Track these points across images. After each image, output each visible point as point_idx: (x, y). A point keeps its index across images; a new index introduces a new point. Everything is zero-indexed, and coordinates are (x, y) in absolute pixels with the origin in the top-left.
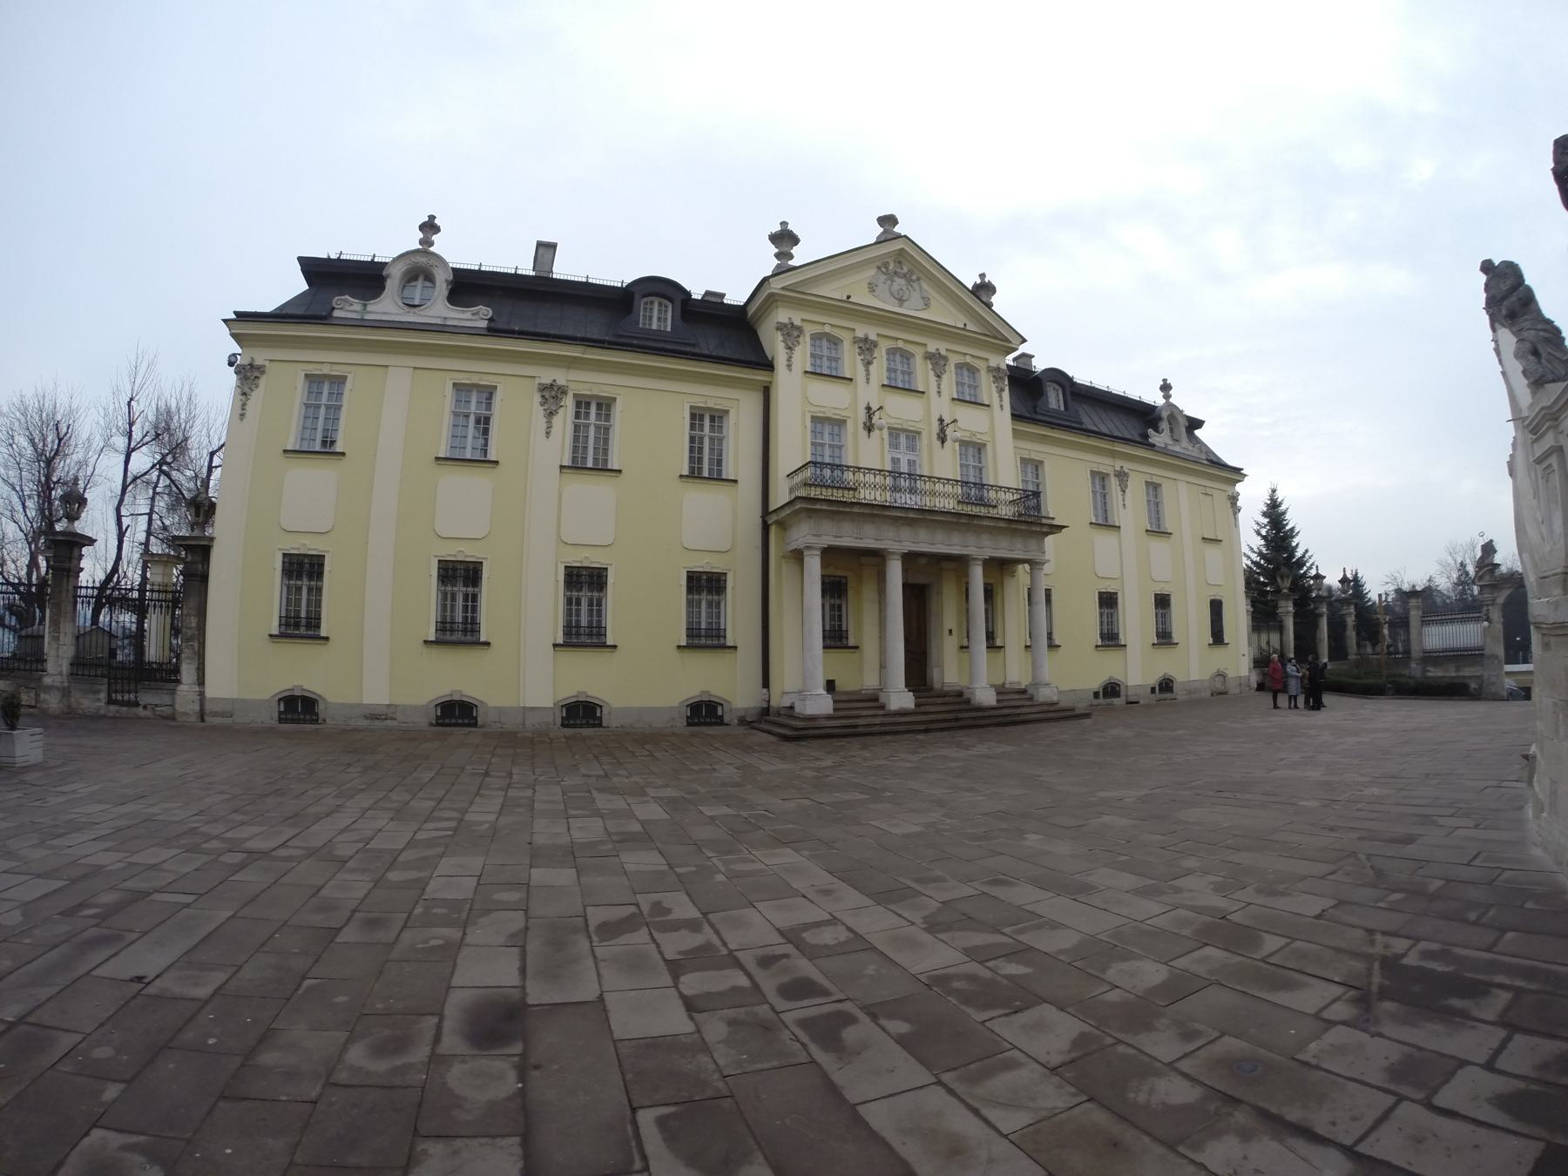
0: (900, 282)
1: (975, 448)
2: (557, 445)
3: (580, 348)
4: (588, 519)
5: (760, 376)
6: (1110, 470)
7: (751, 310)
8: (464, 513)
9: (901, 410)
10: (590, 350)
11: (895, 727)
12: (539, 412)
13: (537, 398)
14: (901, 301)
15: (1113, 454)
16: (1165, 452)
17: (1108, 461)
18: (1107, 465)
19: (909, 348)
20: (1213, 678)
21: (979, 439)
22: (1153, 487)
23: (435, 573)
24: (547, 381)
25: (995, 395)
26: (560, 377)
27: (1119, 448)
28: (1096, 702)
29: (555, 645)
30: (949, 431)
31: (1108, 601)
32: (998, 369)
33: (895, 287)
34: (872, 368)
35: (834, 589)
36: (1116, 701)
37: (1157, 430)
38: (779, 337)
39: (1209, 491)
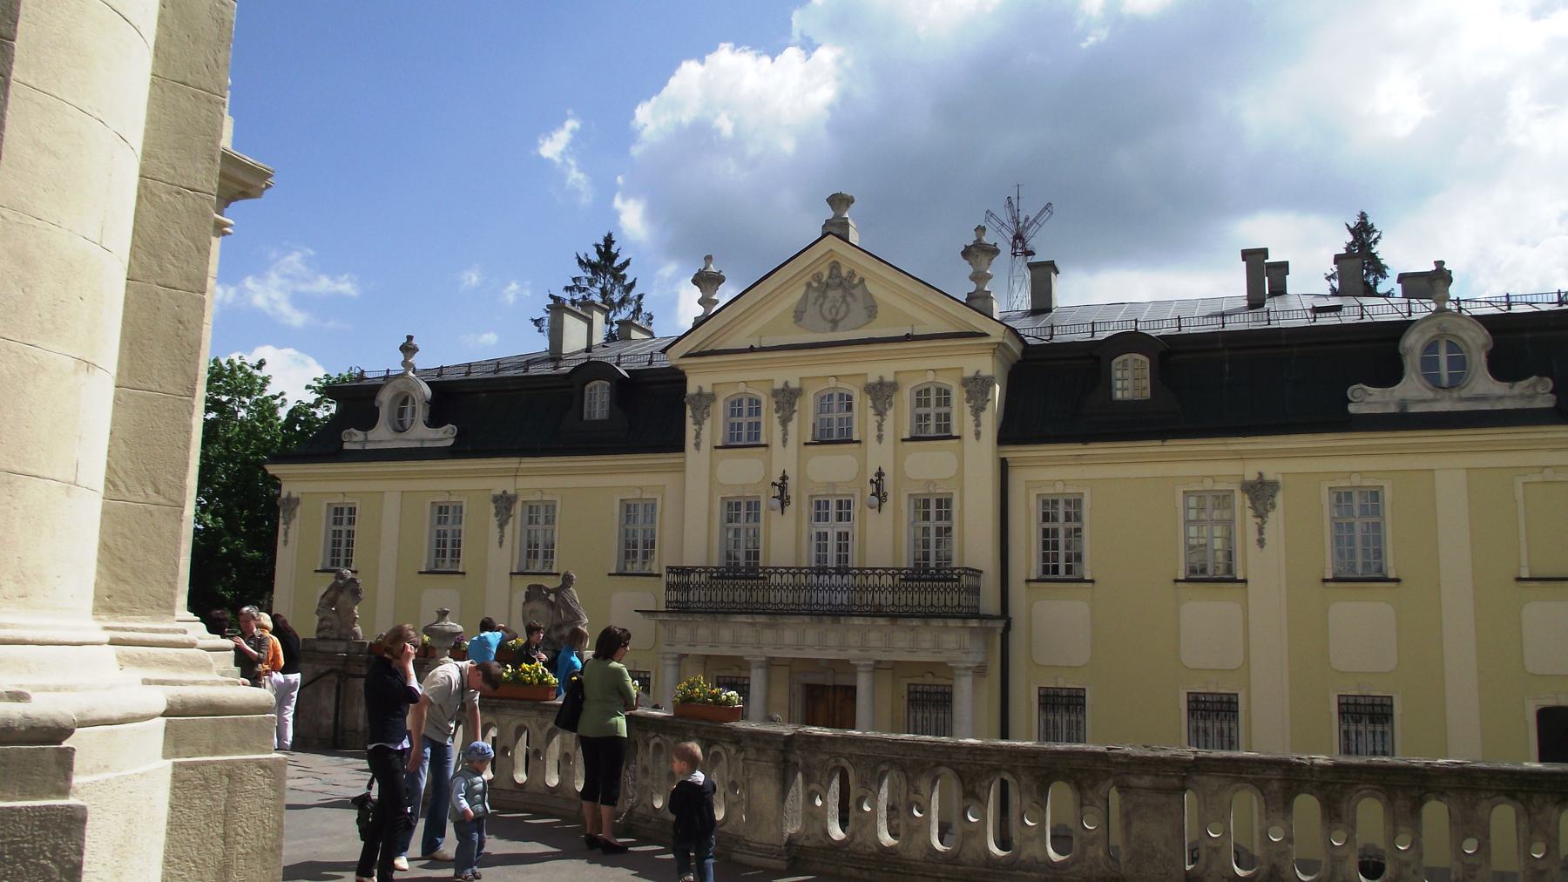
9: (833, 469)
12: (494, 522)
13: (493, 510)
15: (1240, 457)
17: (1233, 468)
19: (846, 386)
21: (941, 490)
24: (499, 492)
33: (827, 305)
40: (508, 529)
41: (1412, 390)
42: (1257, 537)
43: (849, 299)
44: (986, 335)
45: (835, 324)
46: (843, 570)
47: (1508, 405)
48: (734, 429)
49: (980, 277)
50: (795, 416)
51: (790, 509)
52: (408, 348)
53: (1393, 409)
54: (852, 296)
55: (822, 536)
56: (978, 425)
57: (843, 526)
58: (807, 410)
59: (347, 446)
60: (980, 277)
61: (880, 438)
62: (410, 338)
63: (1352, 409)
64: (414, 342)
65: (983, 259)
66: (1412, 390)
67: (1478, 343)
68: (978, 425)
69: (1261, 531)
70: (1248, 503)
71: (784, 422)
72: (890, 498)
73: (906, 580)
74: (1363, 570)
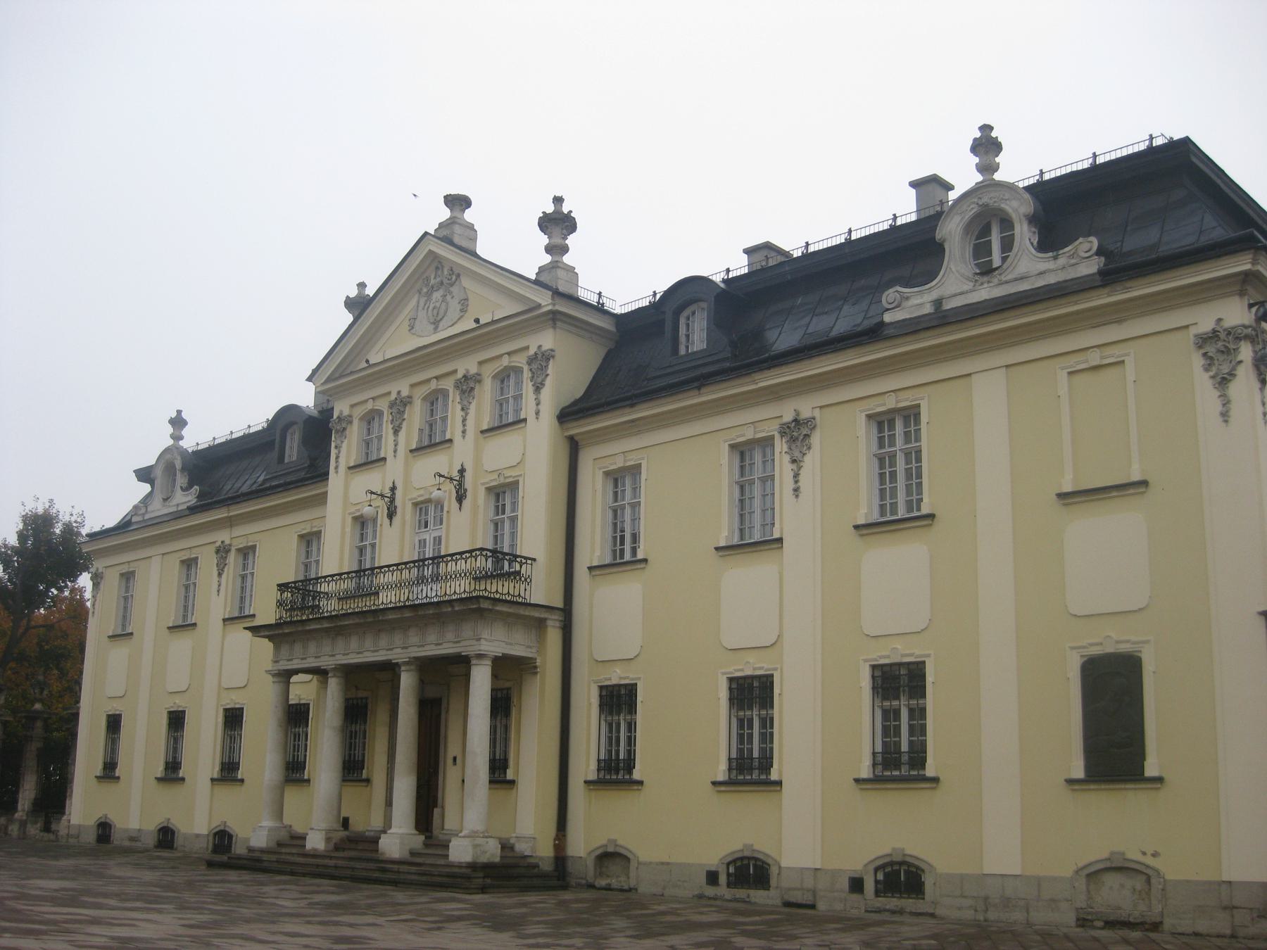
0: (437, 295)
3: (225, 509)
6: (772, 429)
10: (232, 508)
12: (215, 573)
16: (941, 319)
18: (763, 419)
20: (1094, 875)
23: (724, 694)
28: (710, 891)
29: (212, 780)
31: (752, 694)
34: (402, 434)
36: (758, 896)
41: (956, 283)
42: (791, 485)
43: (448, 297)
44: (539, 306)
45: (436, 324)
47: (1051, 279)
49: (556, 250)
50: (404, 424)
51: (397, 520)
52: (178, 422)
53: (928, 309)
54: (450, 293)
55: (422, 543)
58: (416, 416)
60: (556, 250)
62: (179, 412)
64: (184, 415)
65: (557, 231)
66: (956, 283)
67: (1019, 209)
69: (796, 476)
70: (785, 448)
71: (396, 432)
74: (899, 512)
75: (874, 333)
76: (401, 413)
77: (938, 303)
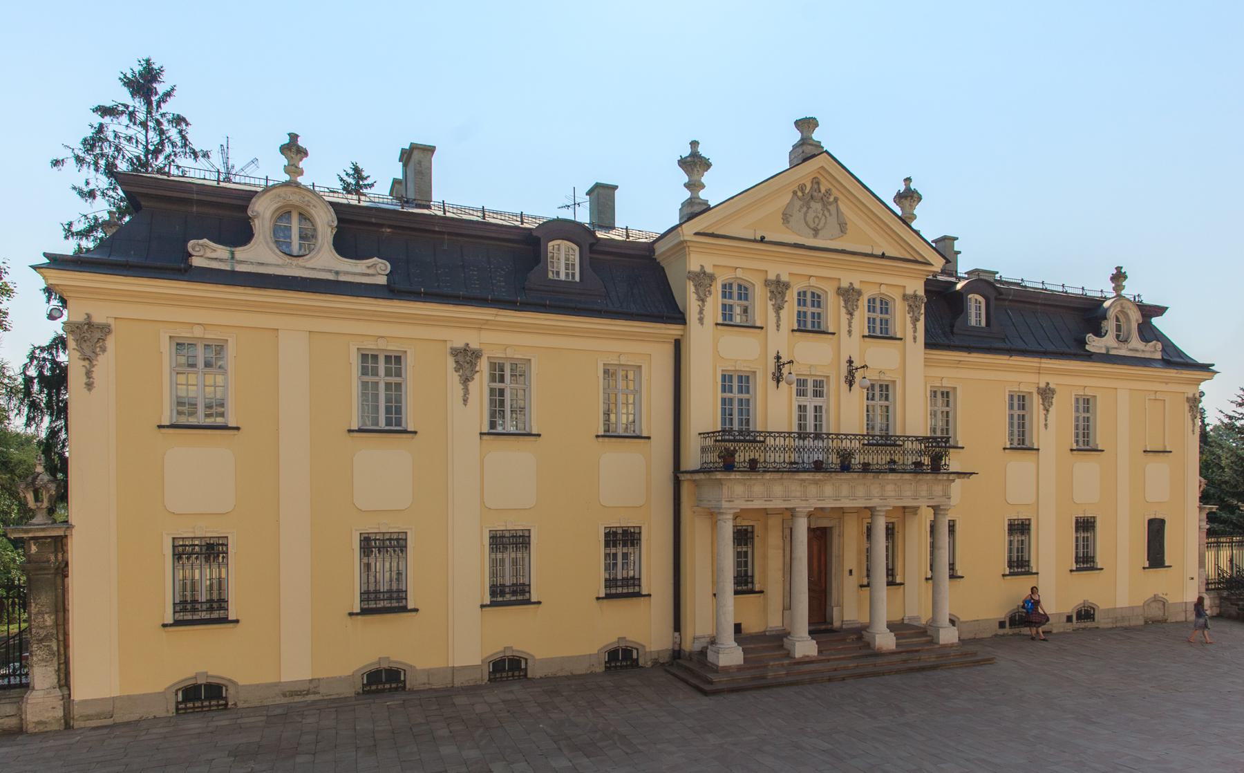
1: (882, 391)
2: (477, 411)
4: (508, 483)
5: (674, 330)
7: (660, 249)
8: (383, 482)
9: (812, 355)
11: (801, 677)
12: (454, 379)
14: (816, 232)
15: (1039, 371)
16: (1107, 358)
17: (1033, 378)
22: (1086, 404)
25: (909, 326)
26: (473, 340)
27: (1047, 363)
30: (858, 375)
32: (915, 296)
34: (782, 313)
35: (743, 537)
37: (1099, 333)
38: (691, 288)
39: (1159, 396)
40: (473, 386)
45: (816, 232)
46: (818, 436)
47: (1147, 356)
48: (727, 310)
50: (786, 305)
53: (1103, 351)
56: (915, 332)
57: (818, 401)
59: (196, 262)
61: (850, 332)
63: (1087, 347)
68: (915, 332)
72: (843, 379)
73: (869, 444)
75: (1090, 357)
76: (783, 294)
77: (1108, 349)
